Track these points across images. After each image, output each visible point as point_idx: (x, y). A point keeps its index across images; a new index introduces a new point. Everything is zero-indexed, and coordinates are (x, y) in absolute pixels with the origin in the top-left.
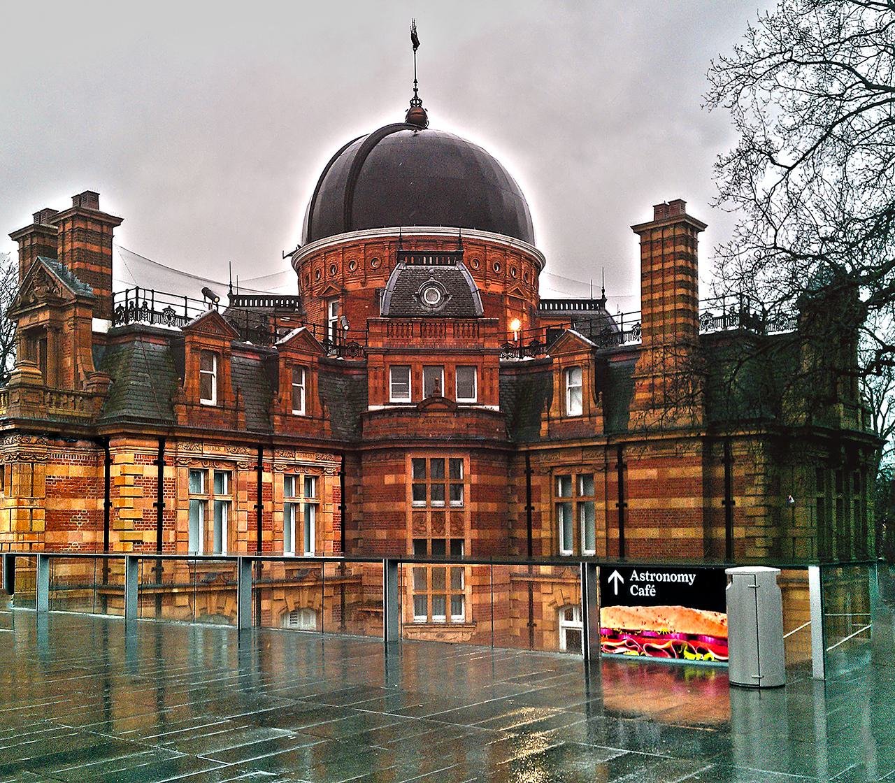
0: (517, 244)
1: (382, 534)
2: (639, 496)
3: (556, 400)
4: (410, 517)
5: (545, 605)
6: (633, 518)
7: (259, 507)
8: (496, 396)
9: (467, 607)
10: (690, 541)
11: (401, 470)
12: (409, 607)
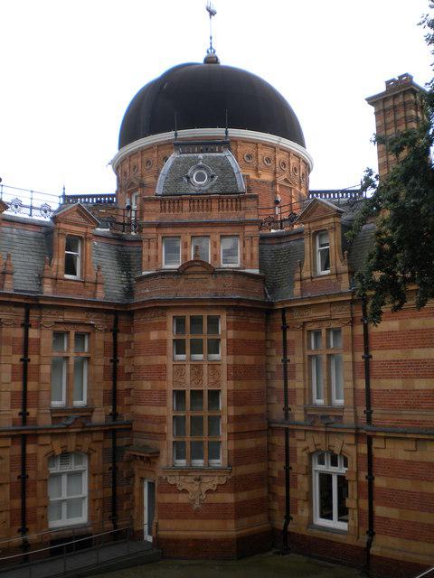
0: (286, 143)
1: (147, 385)
2: (382, 348)
4: (170, 369)
5: (299, 453)
6: (375, 369)
7: (25, 361)
8: (256, 262)
9: (223, 453)
11: (163, 326)
12: (167, 454)
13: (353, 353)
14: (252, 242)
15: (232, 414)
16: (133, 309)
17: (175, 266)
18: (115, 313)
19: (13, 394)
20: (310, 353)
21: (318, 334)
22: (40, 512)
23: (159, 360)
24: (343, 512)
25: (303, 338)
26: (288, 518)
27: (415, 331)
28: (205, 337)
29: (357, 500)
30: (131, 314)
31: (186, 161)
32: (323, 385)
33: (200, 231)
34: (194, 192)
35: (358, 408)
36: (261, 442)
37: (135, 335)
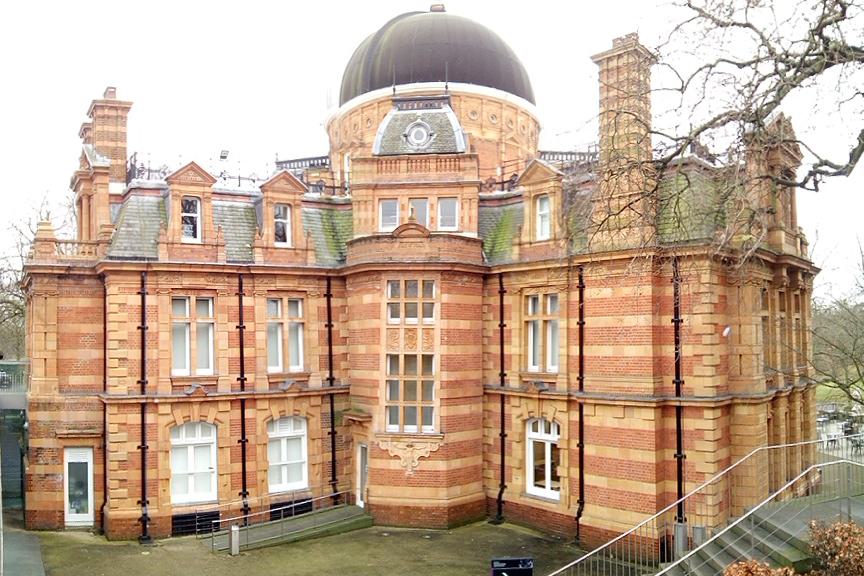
1: (362, 349)
2: (595, 314)
3: (526, 226)
4: (384, 333)
5: (514, 417)
7: (241, 328)
8: (475, 225)
9: (436, 420)
10: (641, 359)
12: (380, 422)
13: (568, 318)
14: (470, 205)
15: (445, 379)
16: (345, 274)
17: (390, 229)
18: (329, 279)
19: (230, 359)
20: (527, 319)
21: (535, 300)
22: (260, 476)
23: (373, 323)
24: (555, 478)
25: (520, 303)
26: (503, 487)
27: (626, 299)
28: (419, 300)
29: (569, 468)
30: (343, 279)
31: (404, 119)
32: (539, 351)
33: (418, 192)
34: (412, 152)
35: (571, 374)
36: (476, 408)
37: (349, 299)
